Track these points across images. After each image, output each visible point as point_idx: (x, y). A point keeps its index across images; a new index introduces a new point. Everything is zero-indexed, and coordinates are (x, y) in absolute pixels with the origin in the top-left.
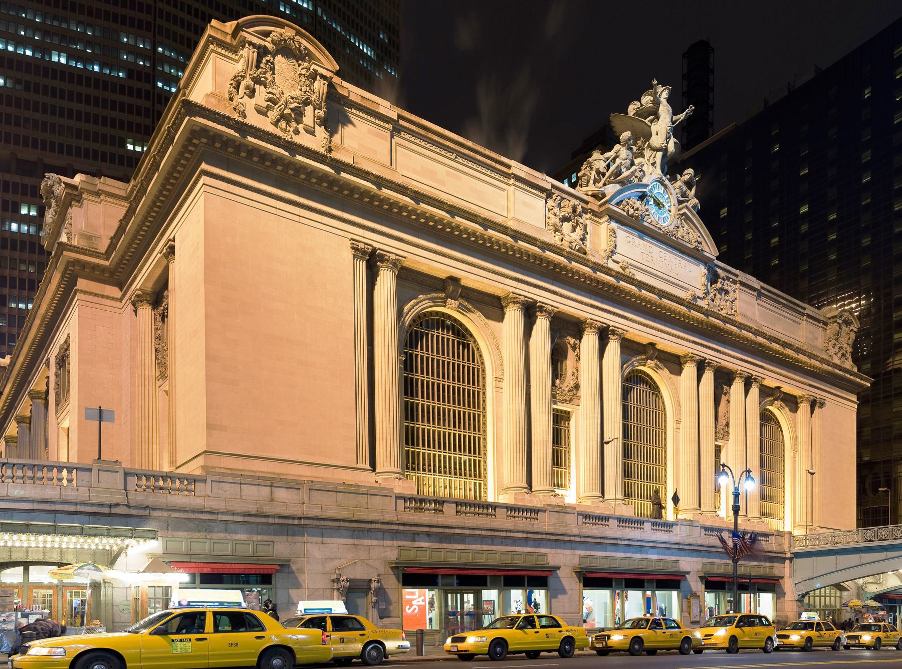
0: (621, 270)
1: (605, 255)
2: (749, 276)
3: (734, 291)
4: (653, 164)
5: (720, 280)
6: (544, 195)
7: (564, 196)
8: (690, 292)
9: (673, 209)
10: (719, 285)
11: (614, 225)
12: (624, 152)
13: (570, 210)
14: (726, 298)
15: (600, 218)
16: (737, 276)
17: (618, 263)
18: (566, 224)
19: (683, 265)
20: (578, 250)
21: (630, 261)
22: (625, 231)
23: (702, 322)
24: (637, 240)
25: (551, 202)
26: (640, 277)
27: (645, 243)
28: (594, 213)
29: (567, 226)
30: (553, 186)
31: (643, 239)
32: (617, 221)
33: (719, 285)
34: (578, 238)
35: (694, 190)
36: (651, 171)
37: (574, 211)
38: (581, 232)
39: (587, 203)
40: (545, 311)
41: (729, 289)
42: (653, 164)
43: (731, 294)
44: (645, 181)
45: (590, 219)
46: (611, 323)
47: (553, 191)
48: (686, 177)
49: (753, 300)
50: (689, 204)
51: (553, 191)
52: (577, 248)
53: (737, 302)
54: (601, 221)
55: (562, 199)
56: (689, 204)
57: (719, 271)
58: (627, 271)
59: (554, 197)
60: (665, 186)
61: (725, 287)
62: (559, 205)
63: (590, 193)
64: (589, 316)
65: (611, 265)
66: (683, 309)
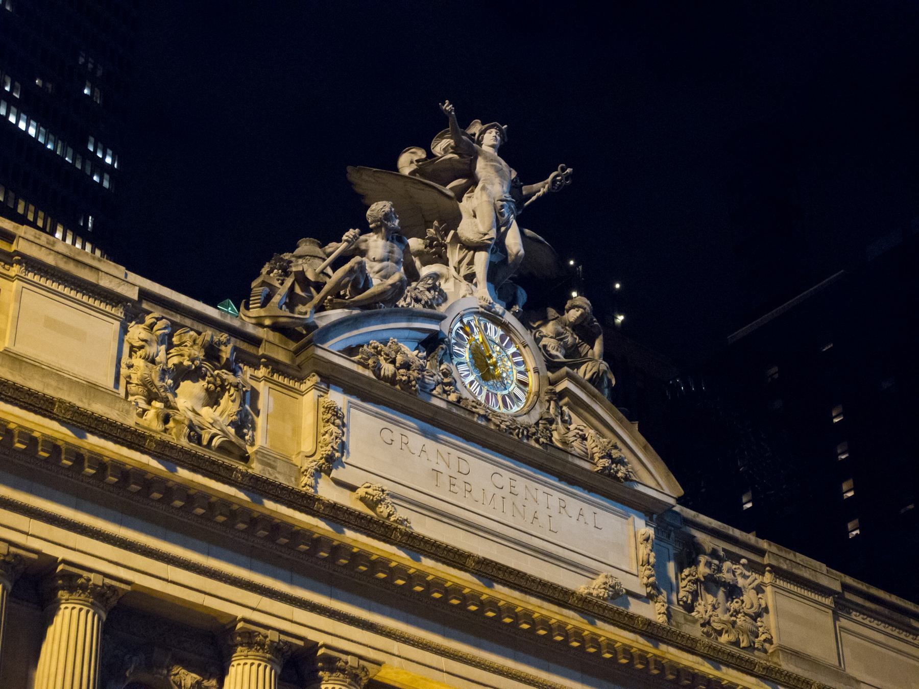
0: (361, 508)
1: (309, 465)
2: (800, 558)
3: (759, 589)
4: (470, 278)
5: (703, 559)
6: (119, 312)
7: (178, 319)
8: (600, 580)
9: (532, 379)
10: (702, 570)
11: (337, 398)
12: (376, 244)
13: (199, 353)
14: (734, 605)
15: (301, 380)
16: (761, 553)
17: (353, 488)
18: (186, 386)
19: (574, 512)
20: (221, 448)
21: (388, 486)
22: (377, 415)
23: (643, 656)
24: (417, 441)
25: (137, 332)
26: (425, 527)
27: (444, 449)
28: (275, 367)
29: (189, 395)
30: (144, 294)
31: (436, 439)
32: (348, 390)
33: (702, 570)
34: (224, 420)
35: (598, 347)
36: (464, 291)
37: (211, 352)
38: (234, 408)
39: (256, 342)
40: (84, 588)
41: (741, 582)
42: (470, 278)
43: (749, 597)
44: (442, 309)
45: (266, 379)
46: (321, 639)
47: (145, 306)
48: (573, 315)
49: (827, 619)
50: (585, 371)
51: (145, 306)
52: (216, 442)
53: (770, 620)
54: (303, 387)
55: (175, 326)
56: (585, 371)
57: (700, 536)
58: (383, 510)
59: (149, 320)
60: (505, 327)
61: (726, 576)
62: (167, 341)
63: (267, 322)
64: (240, 612)
65: (327, 492)
66: (573, 619)
